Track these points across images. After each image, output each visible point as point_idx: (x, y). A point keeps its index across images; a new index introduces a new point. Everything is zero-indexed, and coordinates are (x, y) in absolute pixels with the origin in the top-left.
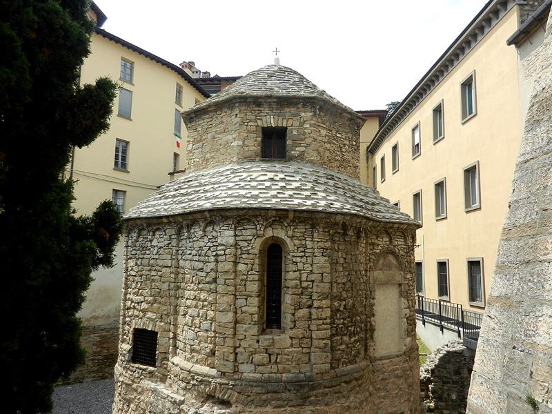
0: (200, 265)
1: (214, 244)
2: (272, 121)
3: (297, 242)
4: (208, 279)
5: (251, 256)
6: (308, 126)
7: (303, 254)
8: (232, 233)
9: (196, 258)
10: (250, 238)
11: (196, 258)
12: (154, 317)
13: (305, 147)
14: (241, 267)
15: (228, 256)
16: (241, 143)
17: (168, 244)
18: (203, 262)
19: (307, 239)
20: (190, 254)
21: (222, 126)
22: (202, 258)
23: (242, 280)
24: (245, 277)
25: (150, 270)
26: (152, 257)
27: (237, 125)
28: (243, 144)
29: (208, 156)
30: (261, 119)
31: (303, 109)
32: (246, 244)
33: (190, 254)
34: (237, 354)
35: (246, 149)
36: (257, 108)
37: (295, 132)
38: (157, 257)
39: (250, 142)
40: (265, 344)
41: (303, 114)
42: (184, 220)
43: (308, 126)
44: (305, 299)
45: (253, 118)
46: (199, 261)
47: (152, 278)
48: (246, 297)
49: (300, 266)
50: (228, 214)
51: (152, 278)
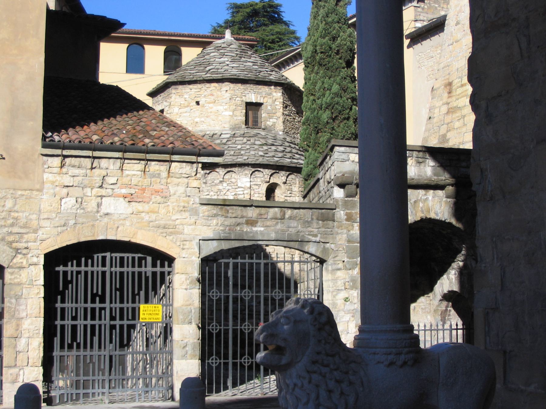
2: (253, 98)
3: (287, 187)
5: (261, 195)
6: (278, 103)
7: (290, 195)
10: (260, 183)
13: (277, 119)
15: (246, 195)
16: (231, 113)
20: (208, 195)
28: (233, 114)
29: (197, 120)
30: (245, 96)
31: (275, 90)
32: (257, 187)
33: (208, 195)
35: (235, 118)
37: (269, 108)
41: (274, 94)
43: (278, 103)
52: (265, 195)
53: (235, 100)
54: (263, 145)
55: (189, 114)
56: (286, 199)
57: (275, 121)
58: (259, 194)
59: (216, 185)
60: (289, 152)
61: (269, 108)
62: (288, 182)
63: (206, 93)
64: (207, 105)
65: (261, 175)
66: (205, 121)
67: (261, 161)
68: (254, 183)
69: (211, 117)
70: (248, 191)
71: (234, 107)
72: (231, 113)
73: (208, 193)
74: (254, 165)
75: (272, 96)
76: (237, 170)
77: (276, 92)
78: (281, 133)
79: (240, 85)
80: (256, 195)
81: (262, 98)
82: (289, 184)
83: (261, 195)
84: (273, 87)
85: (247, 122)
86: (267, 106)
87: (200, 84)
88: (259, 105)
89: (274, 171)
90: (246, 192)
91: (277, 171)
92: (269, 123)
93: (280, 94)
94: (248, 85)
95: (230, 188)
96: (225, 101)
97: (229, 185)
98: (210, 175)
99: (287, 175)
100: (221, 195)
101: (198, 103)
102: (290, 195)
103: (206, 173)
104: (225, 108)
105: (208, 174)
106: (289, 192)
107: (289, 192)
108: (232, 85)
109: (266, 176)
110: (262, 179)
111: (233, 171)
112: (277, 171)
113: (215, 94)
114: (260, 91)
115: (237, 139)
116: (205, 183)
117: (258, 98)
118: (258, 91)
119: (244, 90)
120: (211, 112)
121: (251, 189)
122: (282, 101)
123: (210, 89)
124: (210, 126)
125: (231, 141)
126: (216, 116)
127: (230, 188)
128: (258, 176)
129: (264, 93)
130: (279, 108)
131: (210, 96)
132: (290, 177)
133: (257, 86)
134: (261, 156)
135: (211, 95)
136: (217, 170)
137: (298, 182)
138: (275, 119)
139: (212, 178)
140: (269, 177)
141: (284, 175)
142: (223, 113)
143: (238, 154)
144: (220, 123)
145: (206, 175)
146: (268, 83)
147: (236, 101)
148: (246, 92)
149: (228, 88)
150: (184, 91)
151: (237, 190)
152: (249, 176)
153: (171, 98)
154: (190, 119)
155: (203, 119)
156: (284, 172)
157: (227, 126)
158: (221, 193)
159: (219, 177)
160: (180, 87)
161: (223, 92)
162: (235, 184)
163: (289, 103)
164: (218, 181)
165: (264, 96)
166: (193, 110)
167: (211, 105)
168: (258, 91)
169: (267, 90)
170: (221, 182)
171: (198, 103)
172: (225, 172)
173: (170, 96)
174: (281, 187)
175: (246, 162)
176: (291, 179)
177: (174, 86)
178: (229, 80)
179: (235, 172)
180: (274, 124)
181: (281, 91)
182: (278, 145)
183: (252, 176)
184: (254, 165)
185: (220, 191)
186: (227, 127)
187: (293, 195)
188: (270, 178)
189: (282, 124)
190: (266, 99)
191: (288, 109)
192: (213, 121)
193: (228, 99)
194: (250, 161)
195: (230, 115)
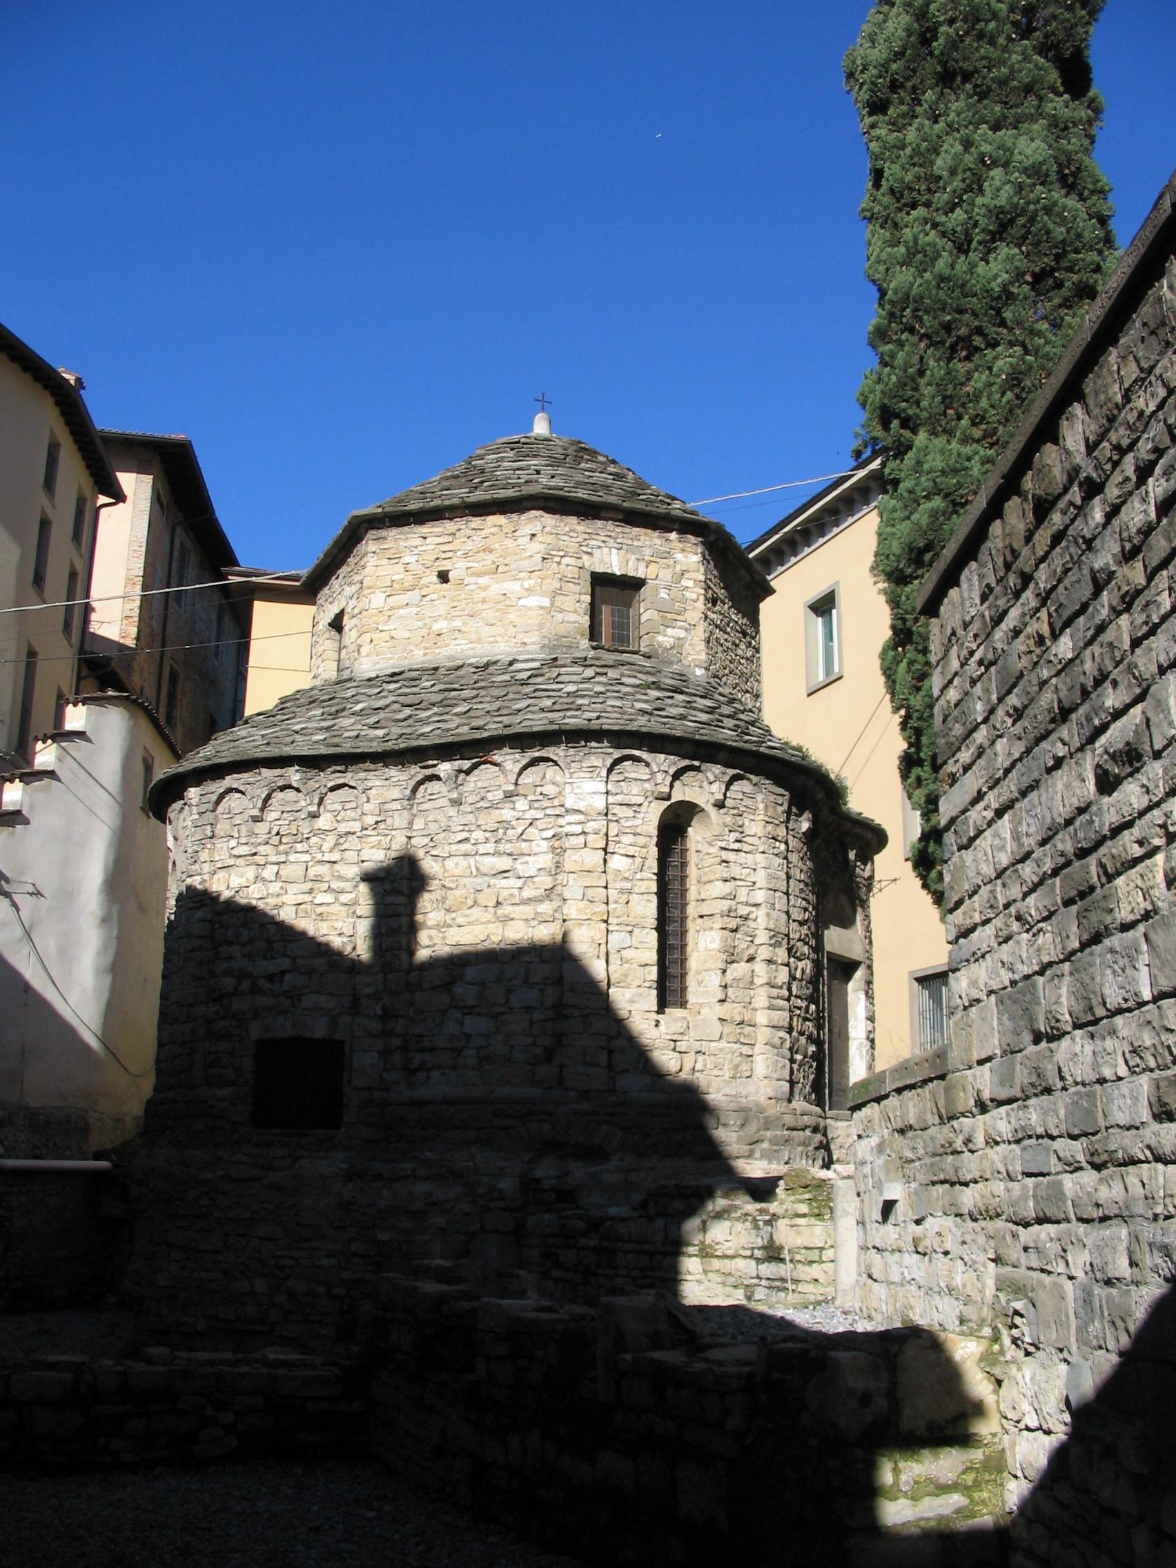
0: (504, 863)
1: (548, 811)
2: (614, 563)
3: (728, 819)
4: (527, 893)
5: (641, 840)
6: (690, 584)
7: (737, 846)
8: (601, 787)
9: (490, 847)
10: (640, 800)
11: (490, 847)
13: (686, 630)
14: (616, 862)
15: (591, 838)
16: (546, 602)
19: (745, 815)
20: (466, 840)
22: (508, 847)
23: (622, 891)
24: (628, 885)
25: (311, 891)
26: (319, 857)
29: (442, 625)
31: (681, 545)
32: (629, 812)
33: (466, 840)
34: (611, 1052)
35: (559, 617)
38: (335, 856)
39: (568, 602)
40: (673, 1030)
41: (679, 556)
43: (690, 584)
44: (741, 942)
45: (573, 548)
46: (497, 853)
47: (319, 910)
48: (630, 928)
49: (736, 871)
51: (319, 910)
52: (655, 839)
53: (559, 563)
54: (648, 686)
55: (415, 610)
56: (724, 857)
57: (682, 634)
58: (635, 834)
59: (493, 806)
60: (729, 716)
61: (663, 594)
62: (729, 803)
63: (469, 546)
64: (473, 580)
65: (641, 772)
66: (463, 629)
67: (641, 724)
68: (619, 798)
69: (484, 614)
70: (601, 823)
71: (557, 584)
72: (546, 602)
73: (465, 835)
74: (620, 738)
75: (671, 562)
76: (562, 754)
77: (683, 550)
78: (699, 672)
79: (573, 520)
80: (626, 839)
81: (642, 565)
82: (735, 812)
83: (641, 840)
84: (673, 536)
85: (594, 632)
86: (656, 589)
87: (451, 519)
88: (632, 585)
89: (687, 762)
90: (590, 827)
91: (696, 763)
92: (666, 639)
93: (698, 558)
94: (599, 523)
95: (539, 814)
96: (527, 564)
97: (536, 805)
98: (471, 778)
99: (727, 778)
100: (510, 841)
101: (444, 577)
102: (737, 846)
103: (460, 771)
104: (526, 584)
105: (468, 772)
106: (733, 836)
107: (733, 836)
108: (550, 520)
109: (659, 777)
110: (647, 785)
111: (547, 760)
112: (696, 763)
113: (497, 546)
114: (636, 543)
115: (563, 670)
116: (457, 803)
117: (631, 563)
118: (630, 542)
119: (587, 536)
120: (484, 601)
121: (610, 817)
122: (703, 578)
123: (483, 533)
124: (479, 641)
125: (542, 675)
126: (498, 611)
127: (539, 814)
128: (634, 775)
129: (648, 552)
130: (694, 596)
131: (481, 554)
132: (736, 787)
133: (628, 529)
134: (644, 712)
135: (484, 550)
136: (497, 757)
137: (761, 806)
138: (680, 628)
139: (479, 784)
140: (669, 779)
141: (717, 779)
142: (521, 602)
143: (566, 706)
144: (512, 631)
145: (462, 776)
146: (662, 523)
147: (563, 566)
148: (592, 542)
149: (536, 527)
150: (403, 544)
151: (561, 821)
152: (604, 773)
153: (364, 567)
154: (420, 624)
155: (457, 623)
156: (717, 769)
157: (533, 639)
158: (510, 832)
159: (501, 779)
160: (393, 533)
161: (521, 541)
162: (556, 803)
163: (721, 593)
164: (500, 795)
165: (647, 558)
166: (428, 598)
167: (483, 581)
168: (630, 542)
169: (658, 542)
170: (509, 796)
171: (444, 577)
172: (524, 762)
173: (362, 563)
174: (708, 816)
175: (595, 725)
176: (741, 797)
177: (374, 532)
178: (541, 503)
179: (556, 763)
180: (679, 643)
181: (700, 550)
182: (695, 695)
183: (613, 777)
184: (620, 738)
185: (505, 824)
186: (533, 643)
187: (746, 848)
188: (672, 786)
189: (702, 646)
190: (653, 567)
191: (717, 608)
192: (487, 628)
193: (538, 558)
194: (607, 724)
195: (542, 608)
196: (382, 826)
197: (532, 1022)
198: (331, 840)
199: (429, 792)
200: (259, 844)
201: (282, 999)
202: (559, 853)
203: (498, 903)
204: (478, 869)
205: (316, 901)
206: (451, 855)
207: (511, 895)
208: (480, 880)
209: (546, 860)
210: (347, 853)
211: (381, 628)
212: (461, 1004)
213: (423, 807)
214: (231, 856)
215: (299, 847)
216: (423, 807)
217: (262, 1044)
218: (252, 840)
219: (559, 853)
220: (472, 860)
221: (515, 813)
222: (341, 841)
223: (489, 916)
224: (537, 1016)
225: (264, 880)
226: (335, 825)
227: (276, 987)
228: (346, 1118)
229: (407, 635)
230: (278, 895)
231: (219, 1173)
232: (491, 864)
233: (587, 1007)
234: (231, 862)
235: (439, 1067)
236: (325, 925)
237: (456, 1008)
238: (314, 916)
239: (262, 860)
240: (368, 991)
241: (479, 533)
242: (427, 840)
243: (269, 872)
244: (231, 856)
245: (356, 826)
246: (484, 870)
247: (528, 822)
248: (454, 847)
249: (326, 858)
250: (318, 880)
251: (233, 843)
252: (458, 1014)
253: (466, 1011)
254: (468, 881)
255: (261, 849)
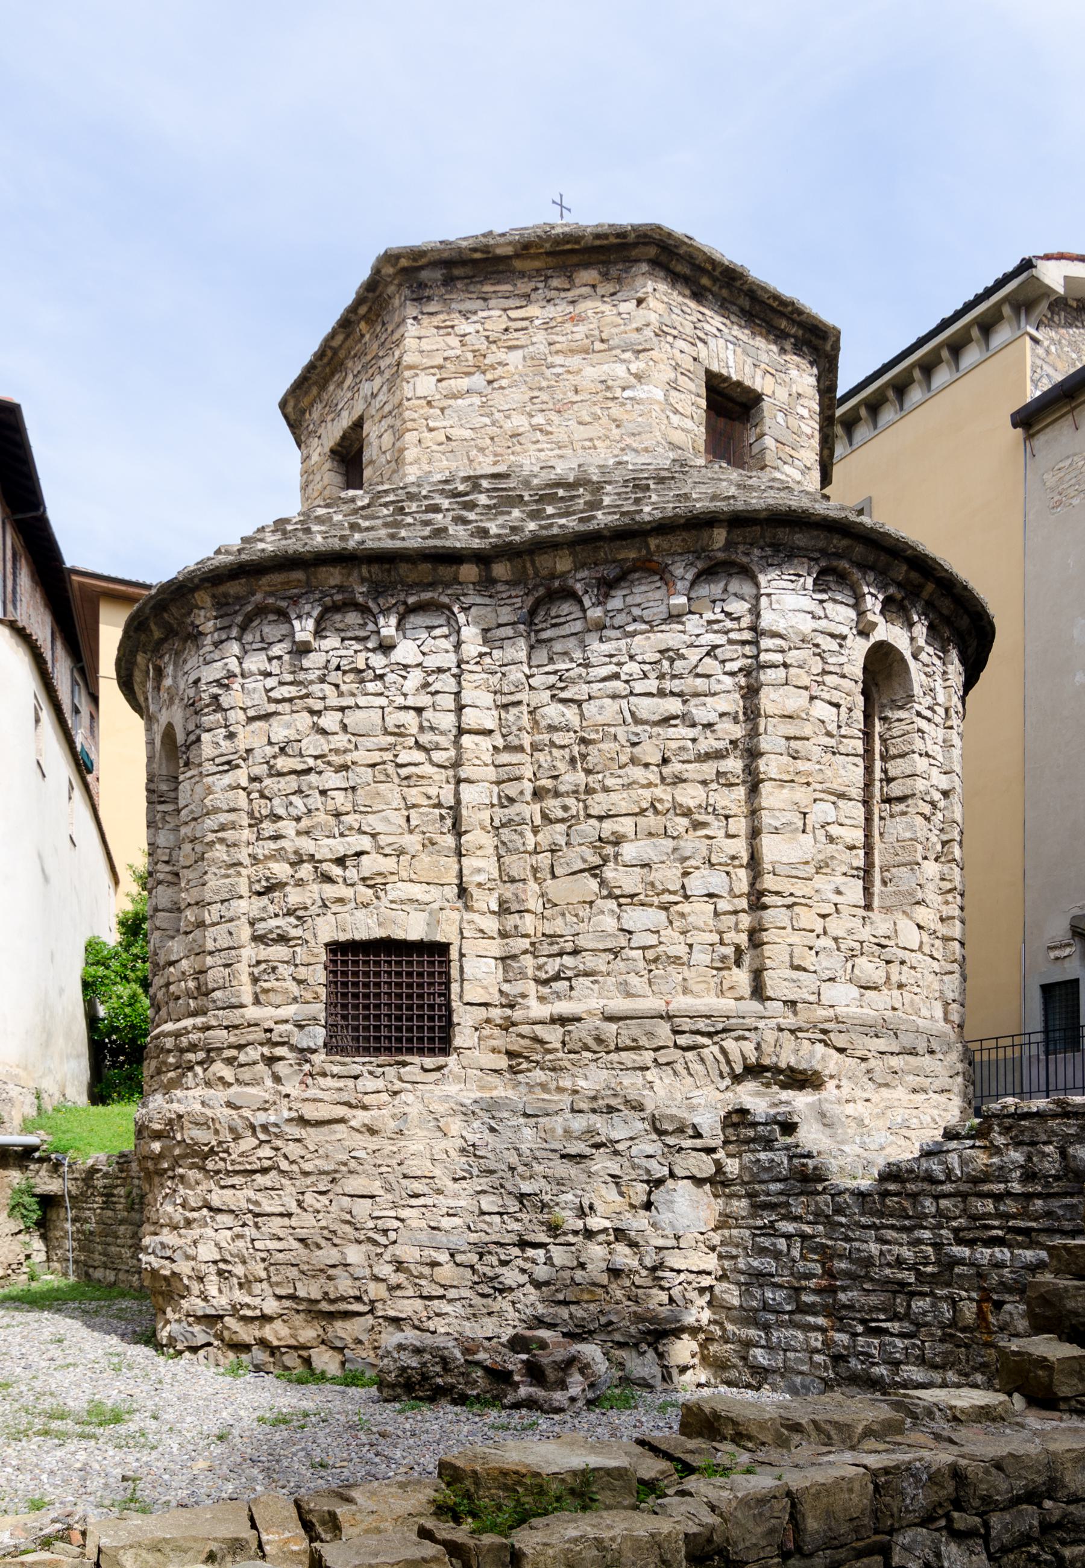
0: (673, 706)
4: (704, 746)
9: (652, 685)
12: (427, 898)
17: (481, 655)
18: (680, 695)
20: (616, 676)
21: (581, 330)
22: (675, 685)
26: (400, 700)
27: (648, 333)
33: (616, 676)
36: (693, 304)
38: (424, 700)
42: (579, 566)
46: (662, 693)
47: (404, 772)
50: (800, 539)
51: (404, 772)
55: (476, 400)
73: (614, 669)
95: (720, 639)
97: (716, 627)
127: (720, 639)
158: (678, 664)
185: (670, 654)
196: (487, 660)
197: (716, 914)
198: (415, 678)
199: (553, 614)
200: (312, 682)
201: (361, 888)
202: (751, 692)
203: (665, 761)
204: (632, 714)
205: (399, 760)
206: (590, 698)
207: (683, 749)
208: (639, 729)
209: (732, 703)
210: (439, 696)
211: (432, 424)
212: (618, 892)
213: (544, 635)
214: (271, 700)
215: (371, 687)
216: (544, 635)
217: (335, 948)
218: (302, 676)
219: (751, 692)
220: (624, 703)
221: (686, 637)
222: (430, 679)
223: (653, 776)
224: (723, 905)
225: (324, 732)
226: (420, 658)
227: (352, 874)
228: (457, 1042)
229: (468, 434)
230: (345, 752)
231: (286, 1114)
232: (648, 708)
233: (792, 895)
234: (272, 707)
235: (586, 974)
236: (414, 791)
237: (610, 896)
238: (396, 780)
239: (318, 705)
240: (481, 878)
241: (563, 295)
242: (553, 679)
243: (330, 721)
244: (271, 700)
245: (449, 661)
246: (643, 714)
247: (704, 650)
248: (596, 686)
249: (410, 702)
250: (399, 732)
251: (271, 682)
252: (612, 904)
253: (622, 900)
254: (621, 731)
255: (315, 688)
